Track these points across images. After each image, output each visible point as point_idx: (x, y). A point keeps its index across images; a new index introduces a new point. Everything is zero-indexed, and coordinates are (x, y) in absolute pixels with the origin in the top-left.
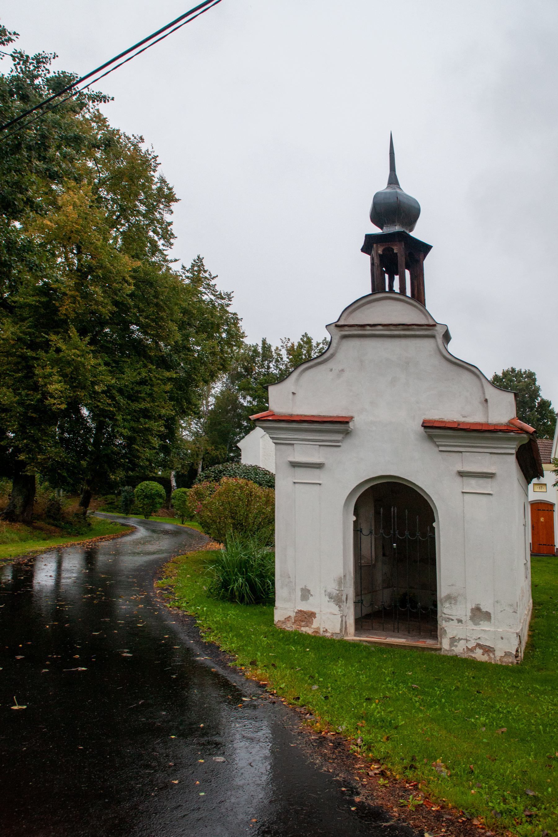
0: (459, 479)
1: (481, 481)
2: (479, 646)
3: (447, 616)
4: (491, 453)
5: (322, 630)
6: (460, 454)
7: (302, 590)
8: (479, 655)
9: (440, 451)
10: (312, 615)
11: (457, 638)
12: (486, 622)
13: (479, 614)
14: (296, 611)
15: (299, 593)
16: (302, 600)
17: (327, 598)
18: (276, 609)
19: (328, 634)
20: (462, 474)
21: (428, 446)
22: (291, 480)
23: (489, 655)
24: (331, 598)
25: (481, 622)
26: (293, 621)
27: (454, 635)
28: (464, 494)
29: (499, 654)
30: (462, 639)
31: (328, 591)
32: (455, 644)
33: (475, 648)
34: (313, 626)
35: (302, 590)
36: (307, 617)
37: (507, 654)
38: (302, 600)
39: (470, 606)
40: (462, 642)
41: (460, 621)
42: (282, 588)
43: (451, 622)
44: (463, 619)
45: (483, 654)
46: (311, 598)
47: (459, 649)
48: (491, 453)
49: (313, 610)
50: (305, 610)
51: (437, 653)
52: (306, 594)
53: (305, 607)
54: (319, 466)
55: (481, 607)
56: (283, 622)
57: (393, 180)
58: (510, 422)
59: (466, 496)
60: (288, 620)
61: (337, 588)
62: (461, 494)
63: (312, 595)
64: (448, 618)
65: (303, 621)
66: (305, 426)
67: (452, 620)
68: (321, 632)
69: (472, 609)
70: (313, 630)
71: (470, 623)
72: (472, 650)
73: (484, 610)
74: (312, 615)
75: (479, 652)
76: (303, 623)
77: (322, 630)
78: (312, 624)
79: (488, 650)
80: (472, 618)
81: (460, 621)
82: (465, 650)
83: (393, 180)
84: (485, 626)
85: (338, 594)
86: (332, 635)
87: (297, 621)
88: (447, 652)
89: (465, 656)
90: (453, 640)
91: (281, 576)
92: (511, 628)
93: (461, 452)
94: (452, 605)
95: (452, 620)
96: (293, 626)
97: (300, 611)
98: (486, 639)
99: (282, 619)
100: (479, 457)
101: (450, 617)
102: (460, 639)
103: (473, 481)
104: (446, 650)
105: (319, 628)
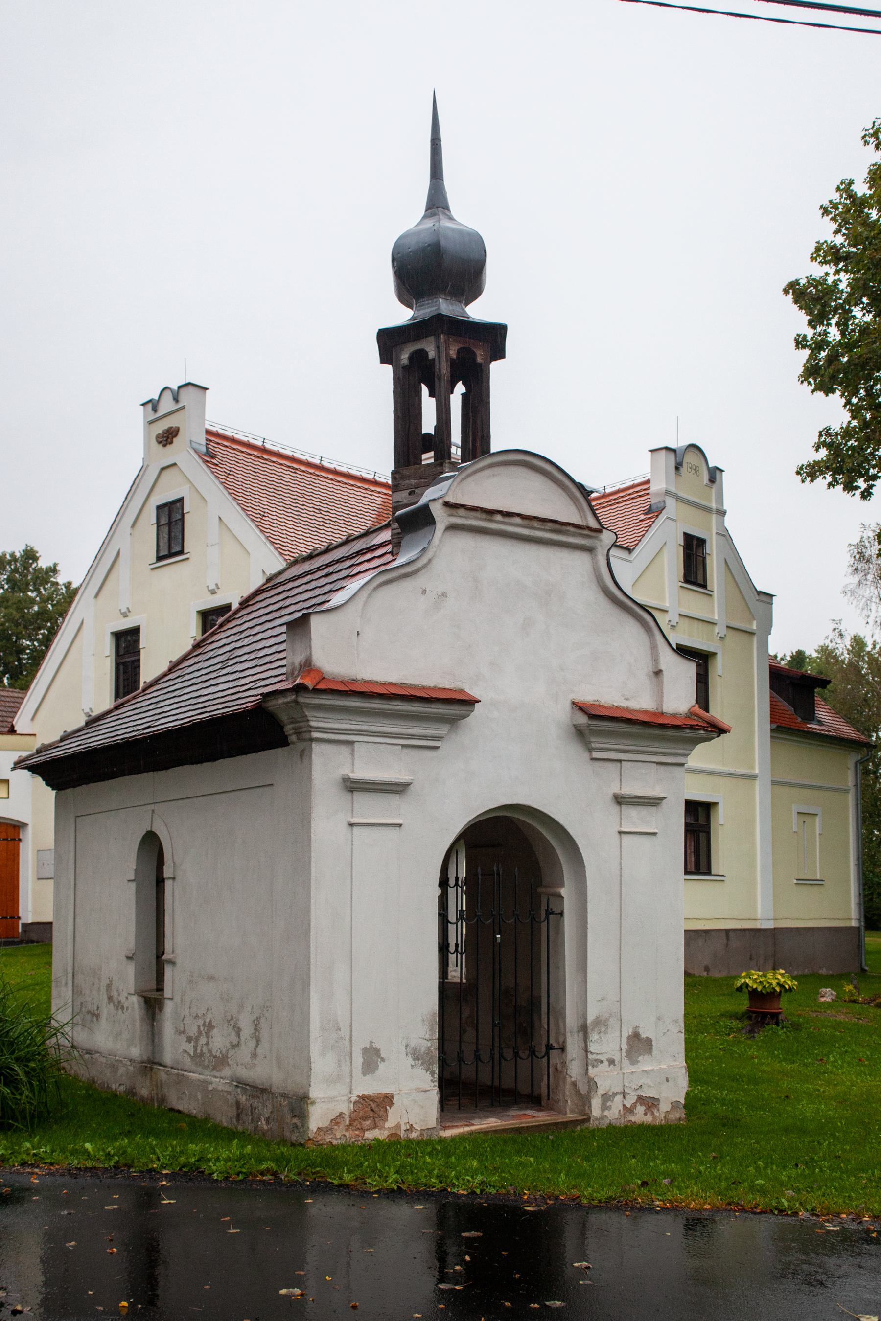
0: (615, 809)
1: (644, 811)
2: (641, 1100)
3: (594, 1056)
4: (658, 763)
5: (403, 1128)
6: (618, 764)
7: (365, 1051)
8: (640, 1116)
9: (593, 759)
10: (387, 1100)
11: (610, 1094)
12: (646, 1056)
13: (639, 1045)
14: (354, 1099)
15: (358, 1060)
16: (365, 1073)
17: (410, 1061)
18: (313, 1103)
19: (414, 1135)
20: (620, 800)
21: (576, 751)
22: (343, 818)
23: (653, 1114)
24: (416, 1058)
25: (640, 1059)
26: (348, 1123)
27: (607, 1089)
28: (623, 835)
29: (664, 1107)
30: (618, 1093)
31: (412, 1045)
32: (608, 1104)
33: (634, 1106)
34: (387, 1125)
35: (365, 1051)
36: (375, 1107)
37: (675, 1105)
38: (365, 1073)
39: (627, 1032)
40: (619, 1098)
41: (611, 1062)
42: (323, 1054)
43: (600, 1065)
44: (617, 1058)
45: (645, 1114)
46: (381, 1066)
47: (614, 1113)
48: (658, 763)
49: (386, 1090)
50: (371, 1094)
51: (586, 1125)
52: (372, 1058)
53: (368, 1087)
54: (398, 789)
55: (641, 1031)
56: (329, 1130)
57: (437, 202)
58: (691, 714)
59: (625, 838)
60: (337, 1124)
61: (427, 1037)
62: (617, 835)
63: (383, 1060)
64: (596, 1060)
65: (365, 1118)
66: (376, 704)
67: (602, 1062)
68: (402, 1134)
69: (629, 1038)
70: (386, 1133)
71: (626, 1061)
72: (629, 1110)
73: (643, 1036)
74: (387, 1100)
75: (640, 1109)
76: (368, 1123)
77: (403, 1128)
78: (386, 1120)
79: (650, 1104)
80: (629, 1054)
81: (611, 1062)
82: (622, 1111)
83: (437, 202)
84: (646, 1064)
85: (429, 1048)
86: (422, 1134)
87: (354, 1120)
88: (597, 1122)
89: (622, 1123)
90: (607, 1098)
91: (323, 1029)
92: (675, 1061)
93: (620, 761)
94: (601, 1034)
95: (602, 1062)
96: (347, 1134)
97: (363, 1098)
98: (649, 1086)
99: (325, 1123)
100: (642, 769)
101: (599, 1057)
102: (615, 1094)
103: (633, 813)
104: (597, 1119)
105: (398, 1126)
